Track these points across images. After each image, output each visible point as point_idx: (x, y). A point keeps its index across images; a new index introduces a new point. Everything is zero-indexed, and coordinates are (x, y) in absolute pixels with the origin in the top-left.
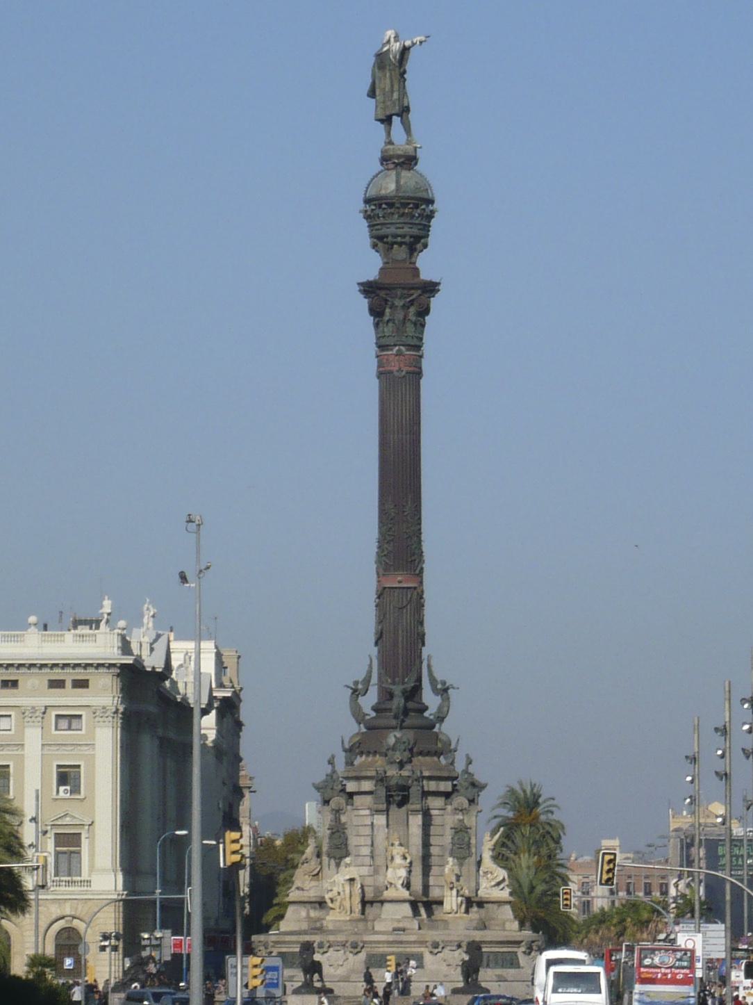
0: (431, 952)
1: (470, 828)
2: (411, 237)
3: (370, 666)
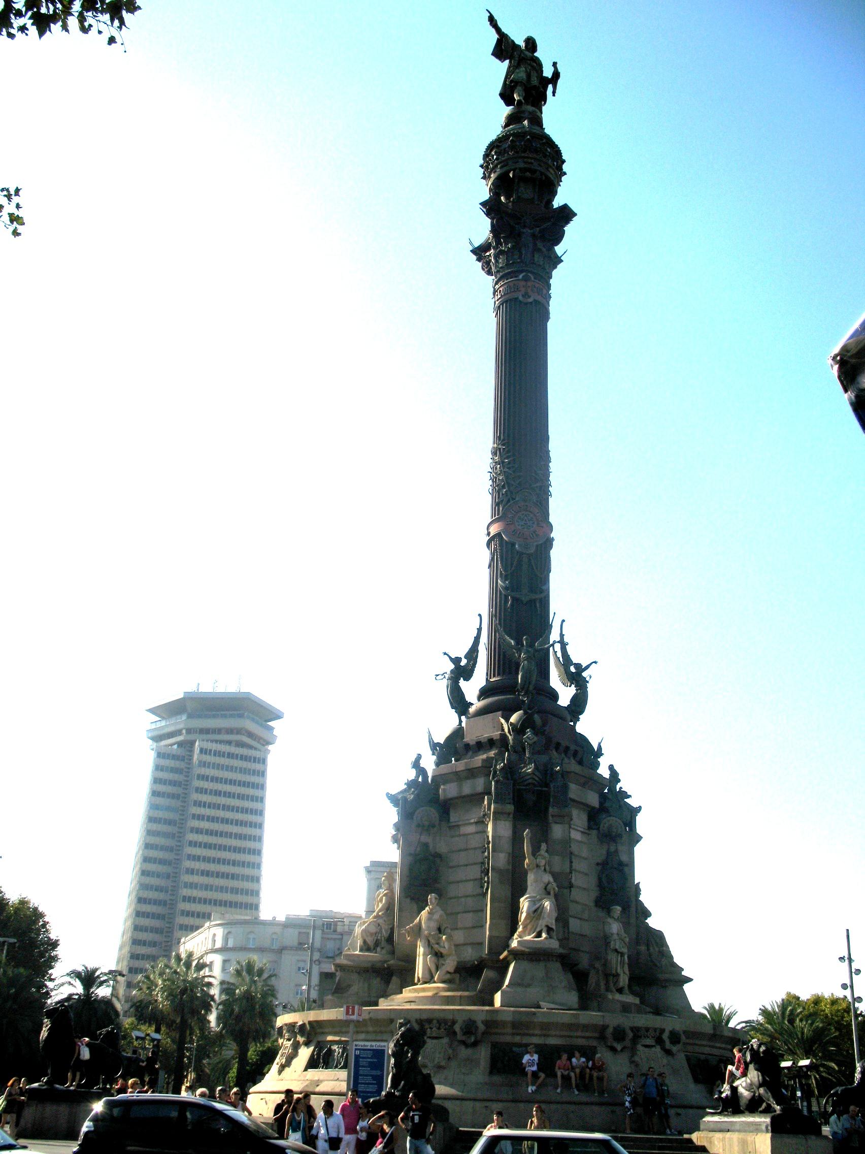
0: (613, 1049)
1: (627, 865)
2: (542, 174)
3: (479, 630)
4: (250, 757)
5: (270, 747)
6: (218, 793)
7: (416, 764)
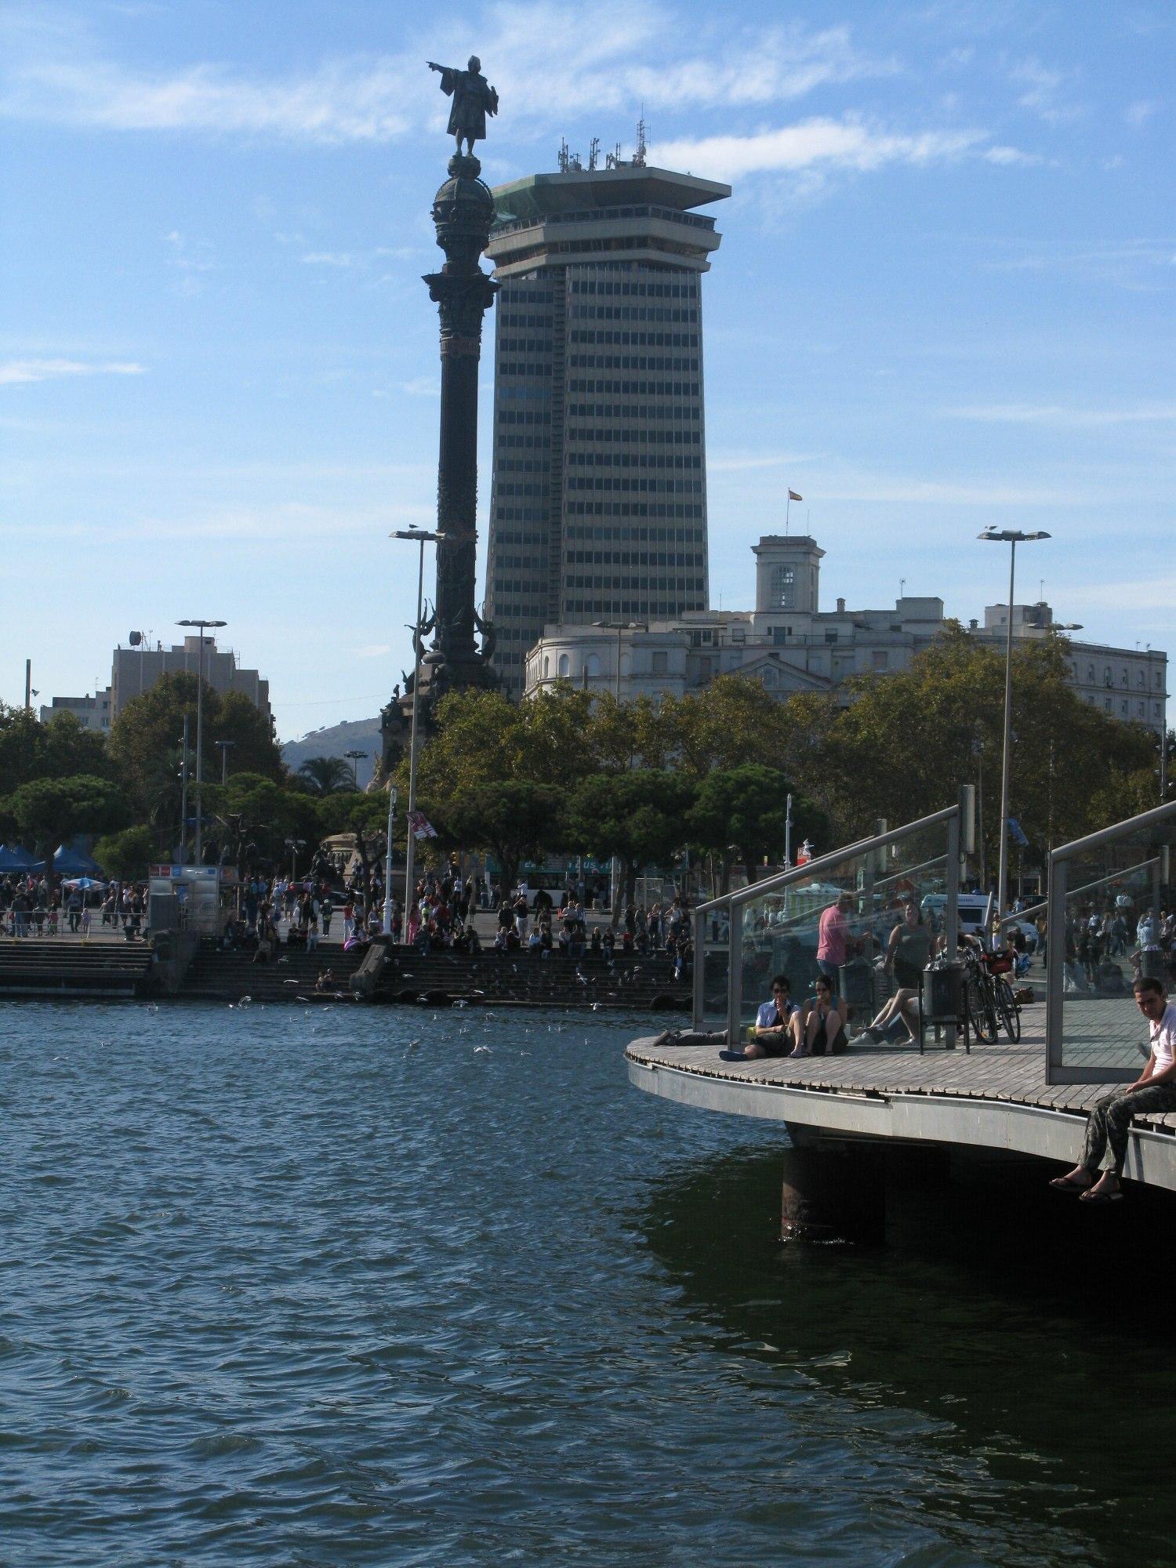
4: (667, 287)
5: (711, 257)
6: (612, 362)
7: (396, 691)
